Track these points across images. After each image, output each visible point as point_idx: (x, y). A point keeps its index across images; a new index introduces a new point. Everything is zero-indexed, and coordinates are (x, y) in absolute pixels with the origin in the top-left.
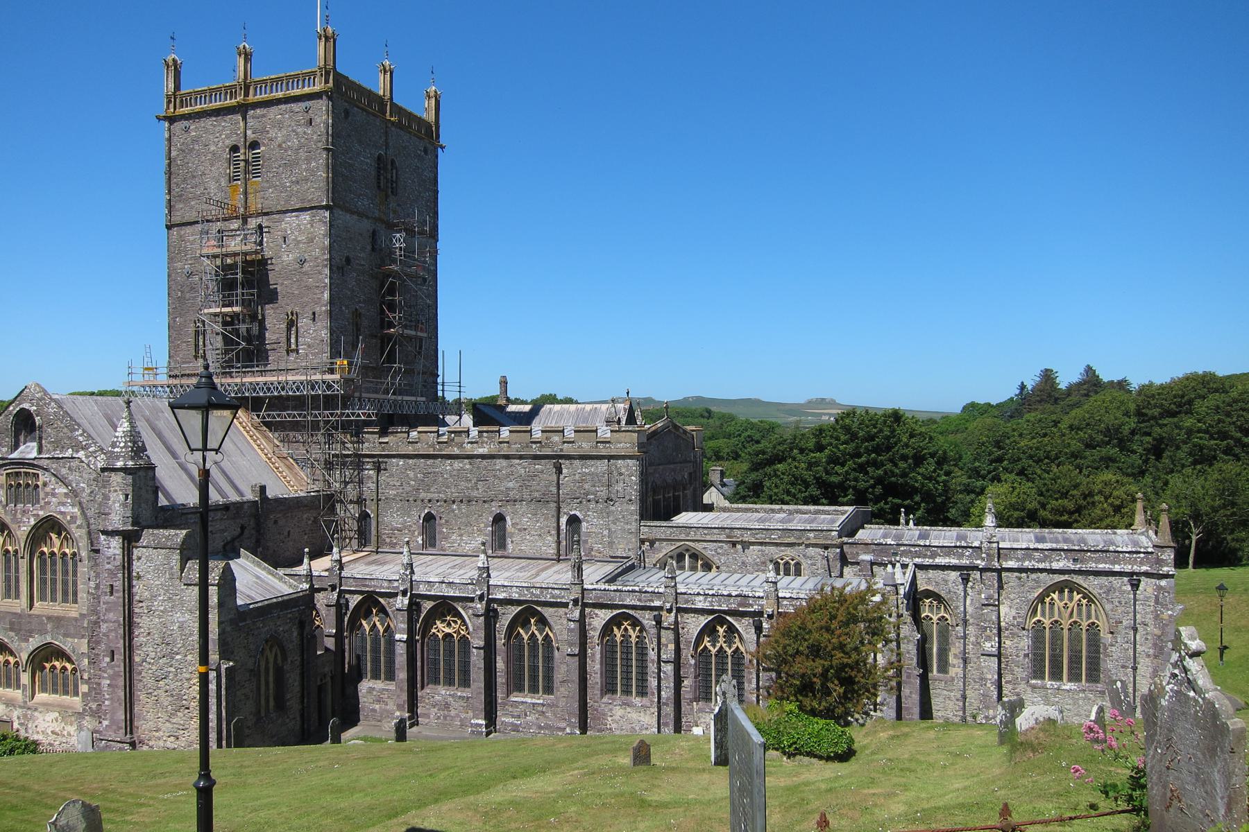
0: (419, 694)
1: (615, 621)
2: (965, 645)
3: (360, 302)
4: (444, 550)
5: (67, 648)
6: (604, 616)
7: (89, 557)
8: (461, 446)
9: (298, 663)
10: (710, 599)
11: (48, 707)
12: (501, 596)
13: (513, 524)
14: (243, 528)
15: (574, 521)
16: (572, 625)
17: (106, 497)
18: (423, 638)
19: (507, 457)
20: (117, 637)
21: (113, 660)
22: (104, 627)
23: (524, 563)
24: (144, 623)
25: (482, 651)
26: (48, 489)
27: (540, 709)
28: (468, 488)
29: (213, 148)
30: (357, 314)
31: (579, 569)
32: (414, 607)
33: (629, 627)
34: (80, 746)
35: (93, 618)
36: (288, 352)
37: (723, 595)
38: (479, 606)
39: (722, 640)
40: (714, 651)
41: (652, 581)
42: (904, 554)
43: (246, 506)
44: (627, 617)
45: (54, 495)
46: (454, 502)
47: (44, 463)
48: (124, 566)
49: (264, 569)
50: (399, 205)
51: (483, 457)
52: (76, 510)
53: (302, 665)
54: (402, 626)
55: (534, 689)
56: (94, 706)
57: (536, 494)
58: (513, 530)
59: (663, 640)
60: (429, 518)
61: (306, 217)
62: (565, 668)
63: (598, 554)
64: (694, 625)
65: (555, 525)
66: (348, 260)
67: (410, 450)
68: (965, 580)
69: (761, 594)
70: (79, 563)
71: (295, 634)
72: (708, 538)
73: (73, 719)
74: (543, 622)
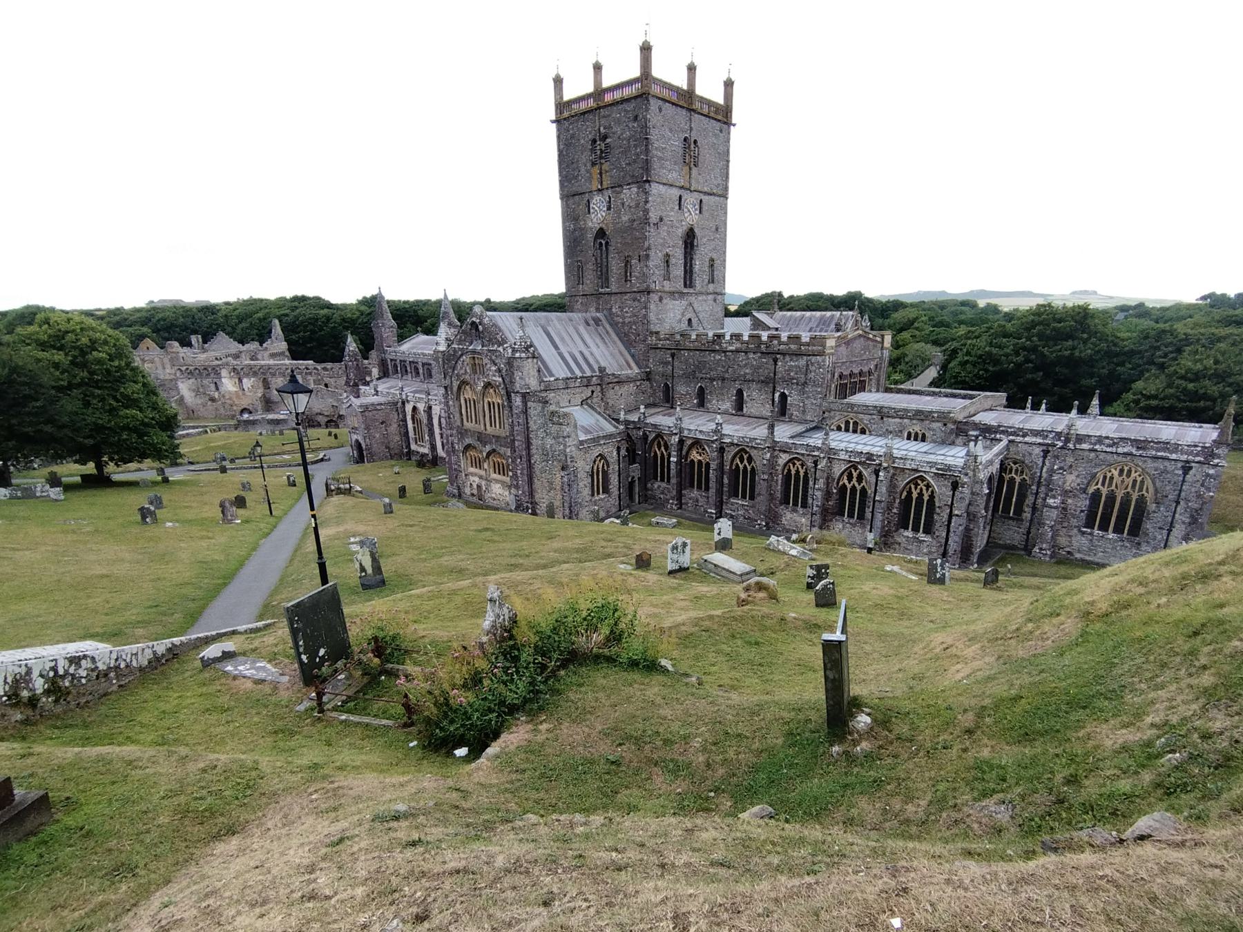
1: (790, 461)
2: (1036, 498)
5: (502, 452)
6: (784, 458)
11: (497, 481)
12: (727, 440)
13: (748, 396)
14: (593, 392)
15: (783, 397)
19: (746, 353)
23: (751, 420)
24: (535, 442)
31: (771, 427)
32: (681, 442)
39: (855, 479)
40: (849, 486)
41: (816, 440)
42: (1003, 432)
44: (799, 460)
49: (602, 416)
51: (732, 351)
52: (500, 379)
55: (744, 497)
60: (701, 390)
64: (838, 469)
68: (1046, 453)
71: (615, 453)
74: (750, 459)
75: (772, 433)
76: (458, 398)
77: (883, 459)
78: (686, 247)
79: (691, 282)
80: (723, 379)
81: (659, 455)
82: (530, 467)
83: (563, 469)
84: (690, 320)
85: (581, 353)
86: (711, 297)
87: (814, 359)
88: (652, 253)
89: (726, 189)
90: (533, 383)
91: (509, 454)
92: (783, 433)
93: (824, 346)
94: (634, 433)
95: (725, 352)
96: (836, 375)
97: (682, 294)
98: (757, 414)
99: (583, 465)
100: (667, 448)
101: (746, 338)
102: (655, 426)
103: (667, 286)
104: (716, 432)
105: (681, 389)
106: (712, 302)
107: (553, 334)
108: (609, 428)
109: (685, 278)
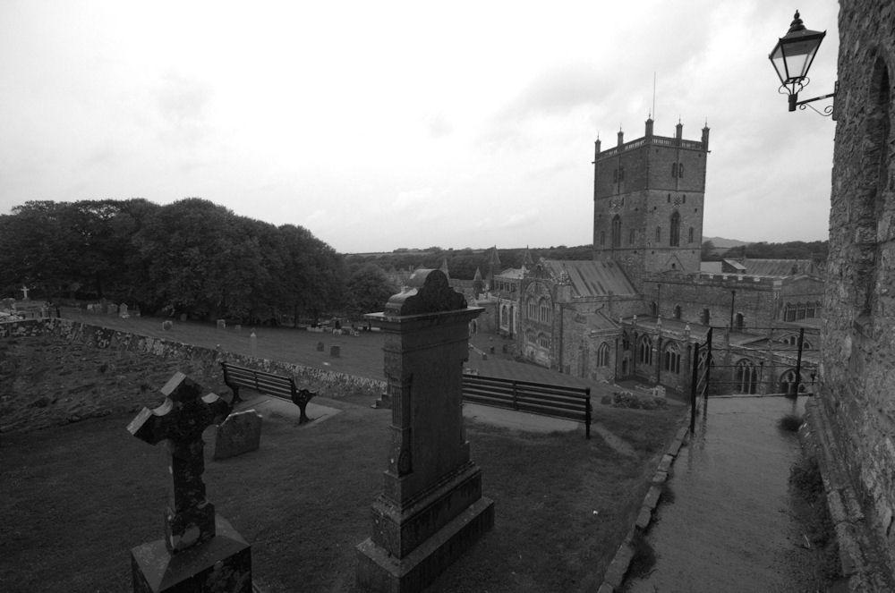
1: (741, 360)
6: (736, 358)
11: (543, 351)
15: (740, 317)
22: (555, 331)
31: (727, 337)
32: (660, 339)
59: (763, 374)
60: (678, 308)
61: (638, 193)
66: (655, 208)
75: (728, 340)
76: (527, 304)
78: (672, 223)
80: (694, 302)
82: (561, 345)
83: (581, 348)
84: (674, 265)
85: (600, 285)
87: (764, 293)
88: (648, 228)
89: (704, 187)
90: (568, 300)
92: (737, 342)
93: (772, 285)
94: (628, 332)
95: (696, 285)
96: (784, 305)
97: (670, 249)
99: (592, 347)
100: (650, 342)
101: (711, 277)
102: (642, 328)
103: (658, 245)
104: (685, 336)
105: (664, 306)
106: (691, 254)
107: (583, 273)
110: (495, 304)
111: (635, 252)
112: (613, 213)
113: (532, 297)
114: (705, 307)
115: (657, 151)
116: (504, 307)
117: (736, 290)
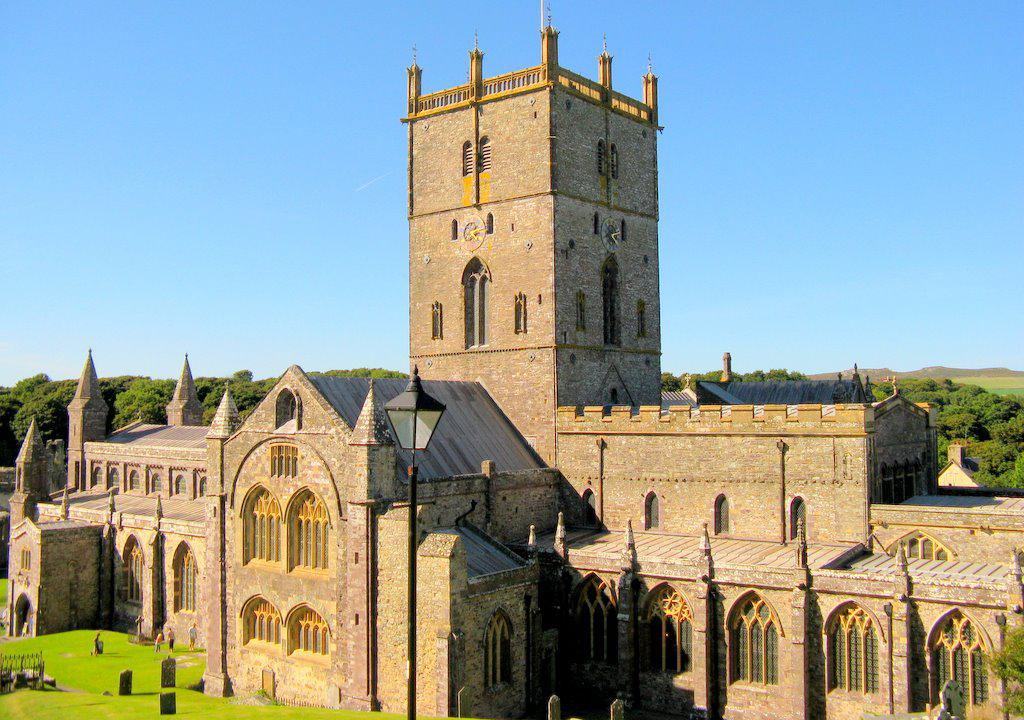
0: (641, 675)
3: (583, 283)
4: (667, 531)
5: (318, 610)
7: (338, 526)
8: (683, 425)
9: (524, 637)
10: (946, 591)
14: (474, 504)
15: (798, 503)
16: (797, 612)
17: (353, 471)
18: (644, 618)
20: (361, 602)
21: (357, 623)
22: (350, 591)
25: (704, 635)
26: (305, 462)
27: (763, 698)
28: (690, 468)
29: (449, 144)
30: (581, 295)
33: (857, 618)
34: (329, 701)
35: (341, 583)
36: (517, 333)
37: (959, 587)
38: (701, 589)
40: (950, 648)
43: (477, 482)
45: (310, 468)
46: (677, 481)
47: (303, 437)
48: (368, 536)
49: (494, 544)
50: (620, 188)
52: (328, 482)
53: (528, 639)
54: (624, 605)
56: (341, 665)
57: (760, 476)
58: (736, 512)
61: (532, 203)
62: (790, 654)
63: (824, 539)
64: (929, 618)
65: (780, 507)
66: (572, 244)
67: (633, 428)
69: (1004, 588)
70: (330, 531)
71: (521, 608)
72: (943, 523)
73: (323, 674)
75: (805, 560)
77: (1006, 596)
79: (612, 335)
81: (592, 611)
84: (614, 392)
85: (451, 441)
86: (642, 358)
89: (655, 207)
91: (333, 610)
98: (752, 535)
106: (644, 366)
108: (509, 565)
109: (605, 327)
110: (98, 531)
111: (533, 359)
112: (463, 253)
113: (261, 491)
114: (717, 490)
115: (569, 105)
116: (132, 542)
117: (785, 440)
